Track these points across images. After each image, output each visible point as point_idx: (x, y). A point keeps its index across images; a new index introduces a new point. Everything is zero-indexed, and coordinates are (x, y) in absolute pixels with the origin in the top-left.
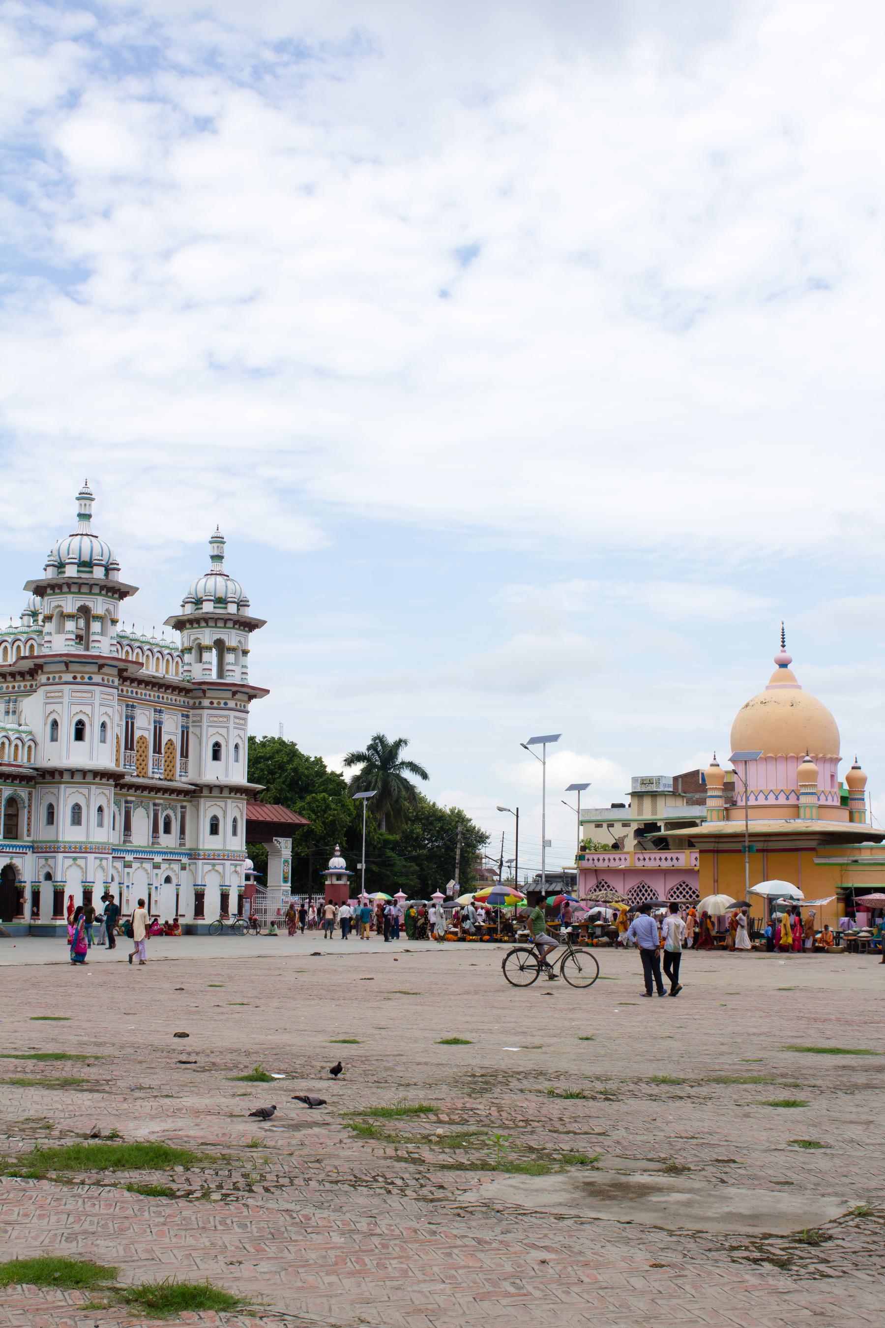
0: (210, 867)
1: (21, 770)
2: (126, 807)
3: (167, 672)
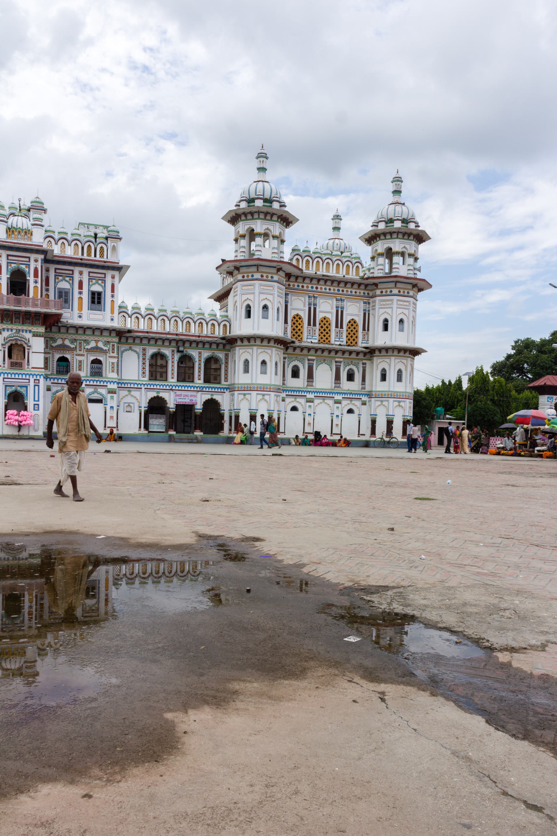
0: (379, 403)
1: (216, 339)
2: (308, 363)
3: (348, 273)
